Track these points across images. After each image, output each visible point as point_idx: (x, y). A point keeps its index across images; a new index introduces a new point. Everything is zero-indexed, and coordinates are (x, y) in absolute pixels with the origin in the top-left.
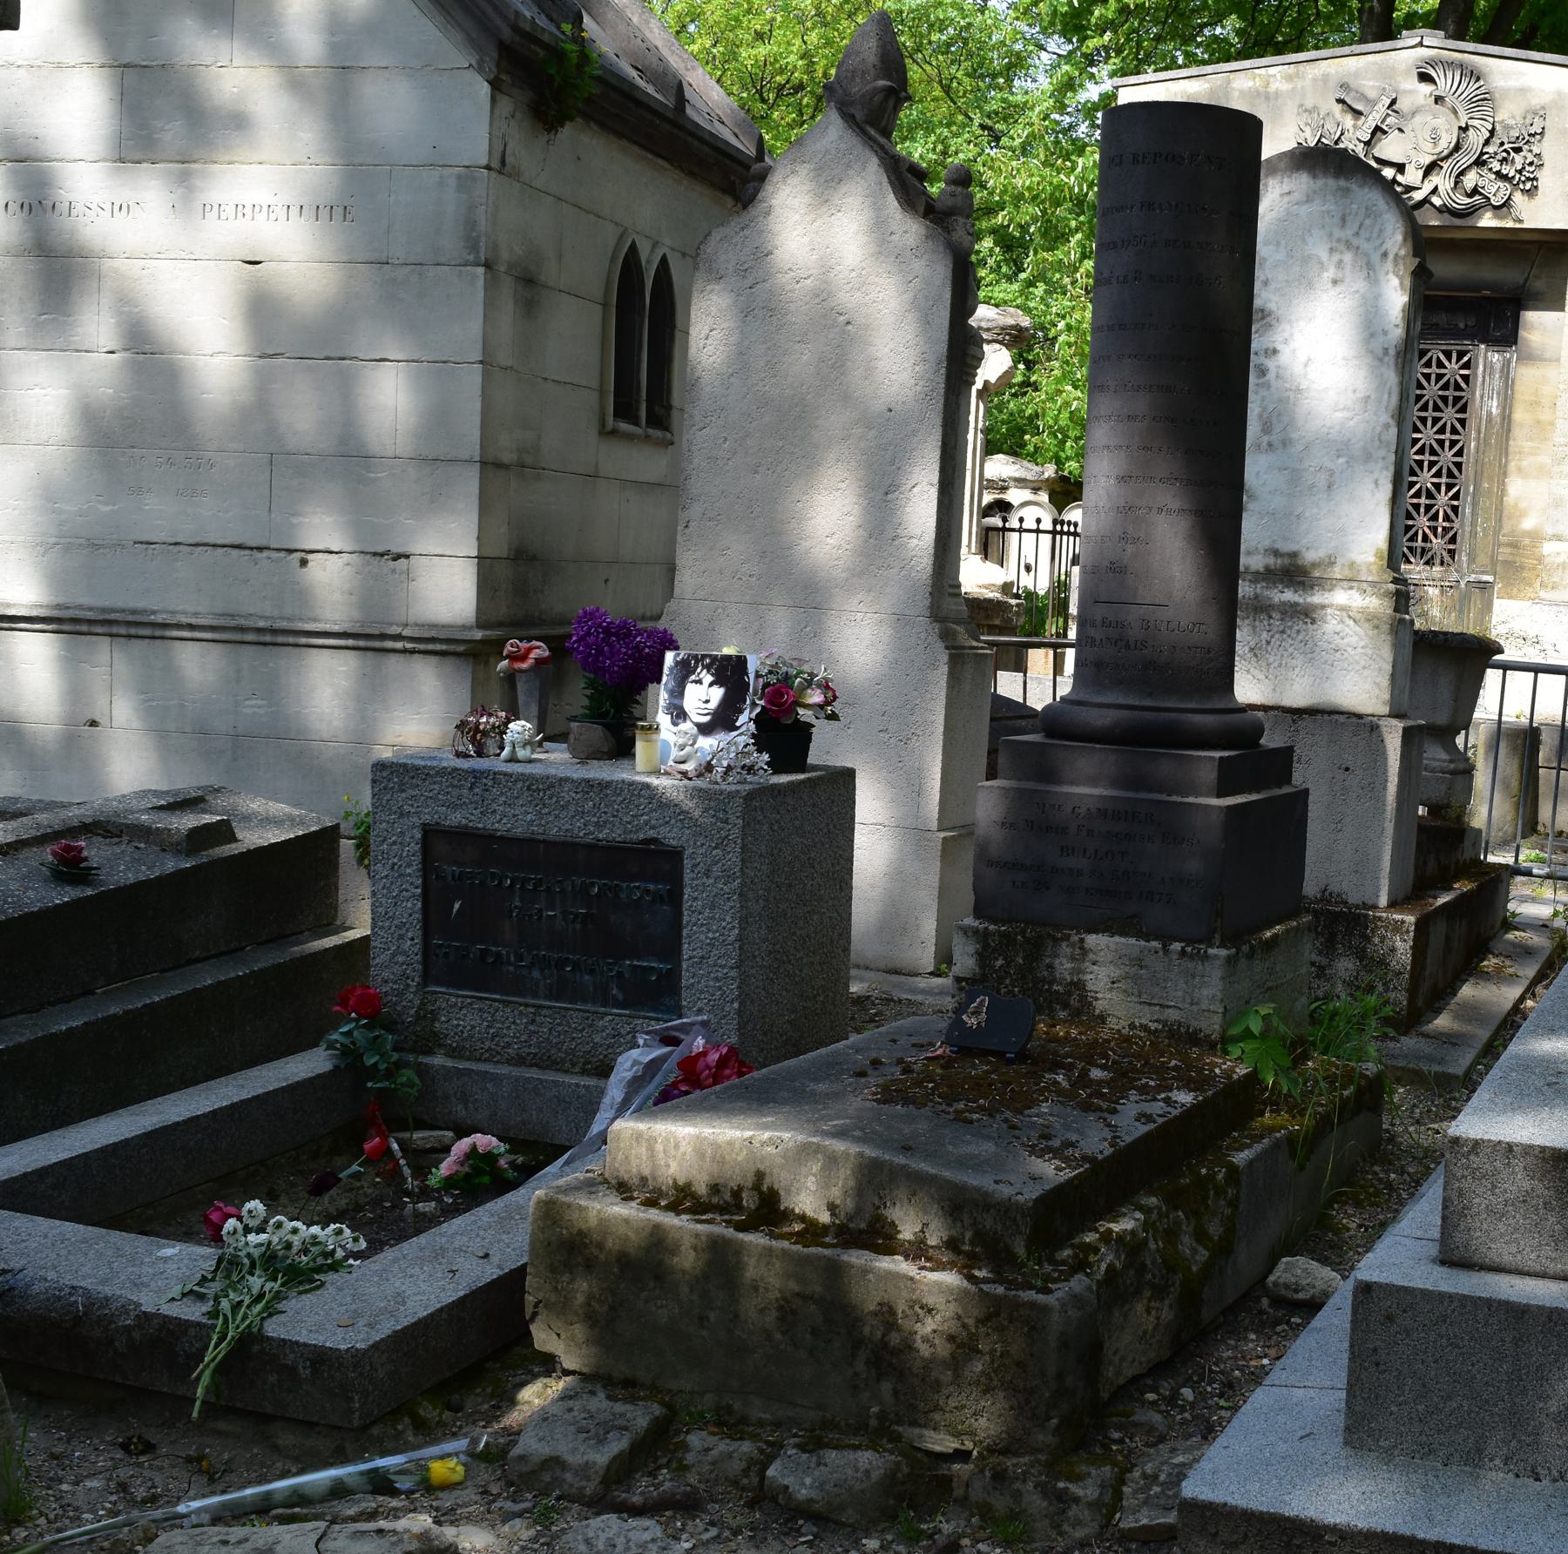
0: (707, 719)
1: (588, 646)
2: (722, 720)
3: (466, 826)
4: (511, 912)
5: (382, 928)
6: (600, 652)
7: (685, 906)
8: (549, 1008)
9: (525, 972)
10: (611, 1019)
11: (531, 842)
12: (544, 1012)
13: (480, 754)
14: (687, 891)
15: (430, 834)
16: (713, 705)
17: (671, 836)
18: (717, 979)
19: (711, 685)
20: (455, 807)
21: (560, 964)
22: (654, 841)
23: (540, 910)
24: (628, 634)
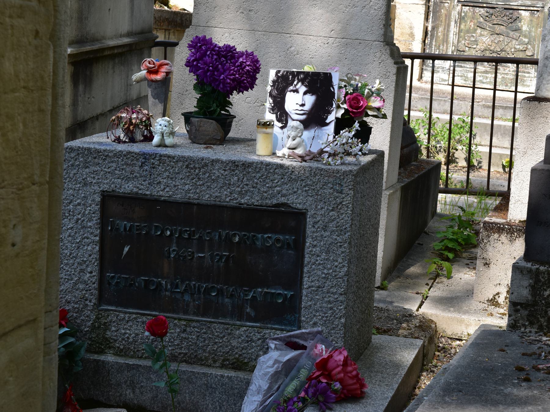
0: (303, 117)
1: (205, 63)
2: (314, 119)
3: (137, 193)
4: (169, 254)
5: (67, 264)
6: (216, 68)
7: (307, 251)
8: (198, 321)
9: (178, 296)
10: (244, 331)
11: (188, 205)
12: (194, 324)
13: (132, 140)
14: (309, 241)
15: (108, 198)
16: (307, 107)
17: (297, 201)
18: (329, 302)
19: (305, 93)
20: (128, 179)
21: (207, 291)
23: (193, 253)
24: (233, 57)
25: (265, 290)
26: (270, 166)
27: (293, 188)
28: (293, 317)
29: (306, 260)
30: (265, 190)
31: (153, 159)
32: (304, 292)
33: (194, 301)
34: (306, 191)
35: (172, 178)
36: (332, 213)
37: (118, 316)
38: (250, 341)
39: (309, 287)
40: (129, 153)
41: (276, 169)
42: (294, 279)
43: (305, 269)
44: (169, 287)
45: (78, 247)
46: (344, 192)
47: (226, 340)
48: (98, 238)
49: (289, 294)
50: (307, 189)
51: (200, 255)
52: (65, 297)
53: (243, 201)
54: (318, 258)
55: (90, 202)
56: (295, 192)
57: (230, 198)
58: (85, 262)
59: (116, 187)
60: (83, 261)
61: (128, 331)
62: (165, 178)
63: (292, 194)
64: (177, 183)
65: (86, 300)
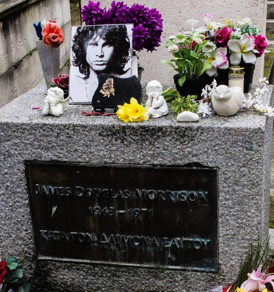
3: (56, 161)
5: (5, 224)
22: (197, 164)
25: (184, 239)
26: (179, 130)
27: (203, 148)
28: (211, 260)
29: (221, 211)
30: (176, 152)
31: (68, 129)
32: (220, 240)
33: (120, 250)
34: (216, 150)
35: (87, 146)
36: (243, 168)
37: (55, 264)
38: (173, 281)
39: (225, 235)
40: (45, 125)
41: (185, 132)
42: (209, 228)
43: (220, 220)
44: (96, 239)
45: (12, 210)
46: (254, 148)
47: (152, 282)
48: (27, 201)
49: (206, 241)
50: (217, 148)
51: (121, 211)
52: (7, 251)
53: (156, 162)
54: (232, 210)
55: (16, 171)
56: (205, 152)
57: (143, 160)
58: (20, 222)
59: (37, 156)
60: (17, 221)
61: (65, 277)
62: (81, 146)
63: (202, 154)
64: (93, 150)
65: (26, 253)
